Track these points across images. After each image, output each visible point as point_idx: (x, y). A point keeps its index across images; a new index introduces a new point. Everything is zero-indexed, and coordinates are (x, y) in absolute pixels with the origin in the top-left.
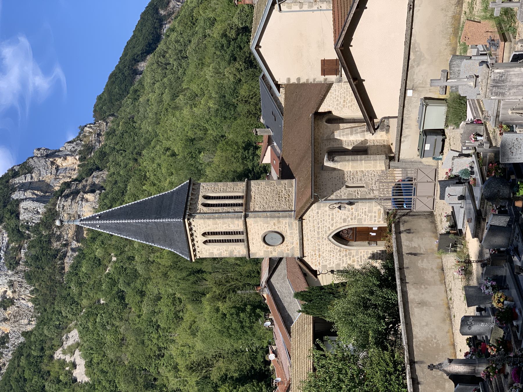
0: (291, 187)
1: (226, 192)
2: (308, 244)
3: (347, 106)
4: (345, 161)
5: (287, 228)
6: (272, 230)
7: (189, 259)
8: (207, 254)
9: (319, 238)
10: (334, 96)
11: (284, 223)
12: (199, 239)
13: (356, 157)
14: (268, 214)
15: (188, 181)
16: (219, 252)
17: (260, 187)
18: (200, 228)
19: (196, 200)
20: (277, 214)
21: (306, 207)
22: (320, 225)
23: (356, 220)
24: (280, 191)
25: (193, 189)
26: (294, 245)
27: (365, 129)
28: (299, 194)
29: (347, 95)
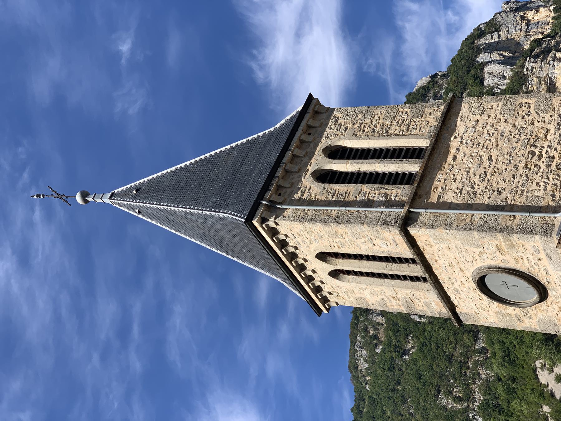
6: (497, 263)
11: (530, 250)
14: (478, 215)
20: (503, 218)
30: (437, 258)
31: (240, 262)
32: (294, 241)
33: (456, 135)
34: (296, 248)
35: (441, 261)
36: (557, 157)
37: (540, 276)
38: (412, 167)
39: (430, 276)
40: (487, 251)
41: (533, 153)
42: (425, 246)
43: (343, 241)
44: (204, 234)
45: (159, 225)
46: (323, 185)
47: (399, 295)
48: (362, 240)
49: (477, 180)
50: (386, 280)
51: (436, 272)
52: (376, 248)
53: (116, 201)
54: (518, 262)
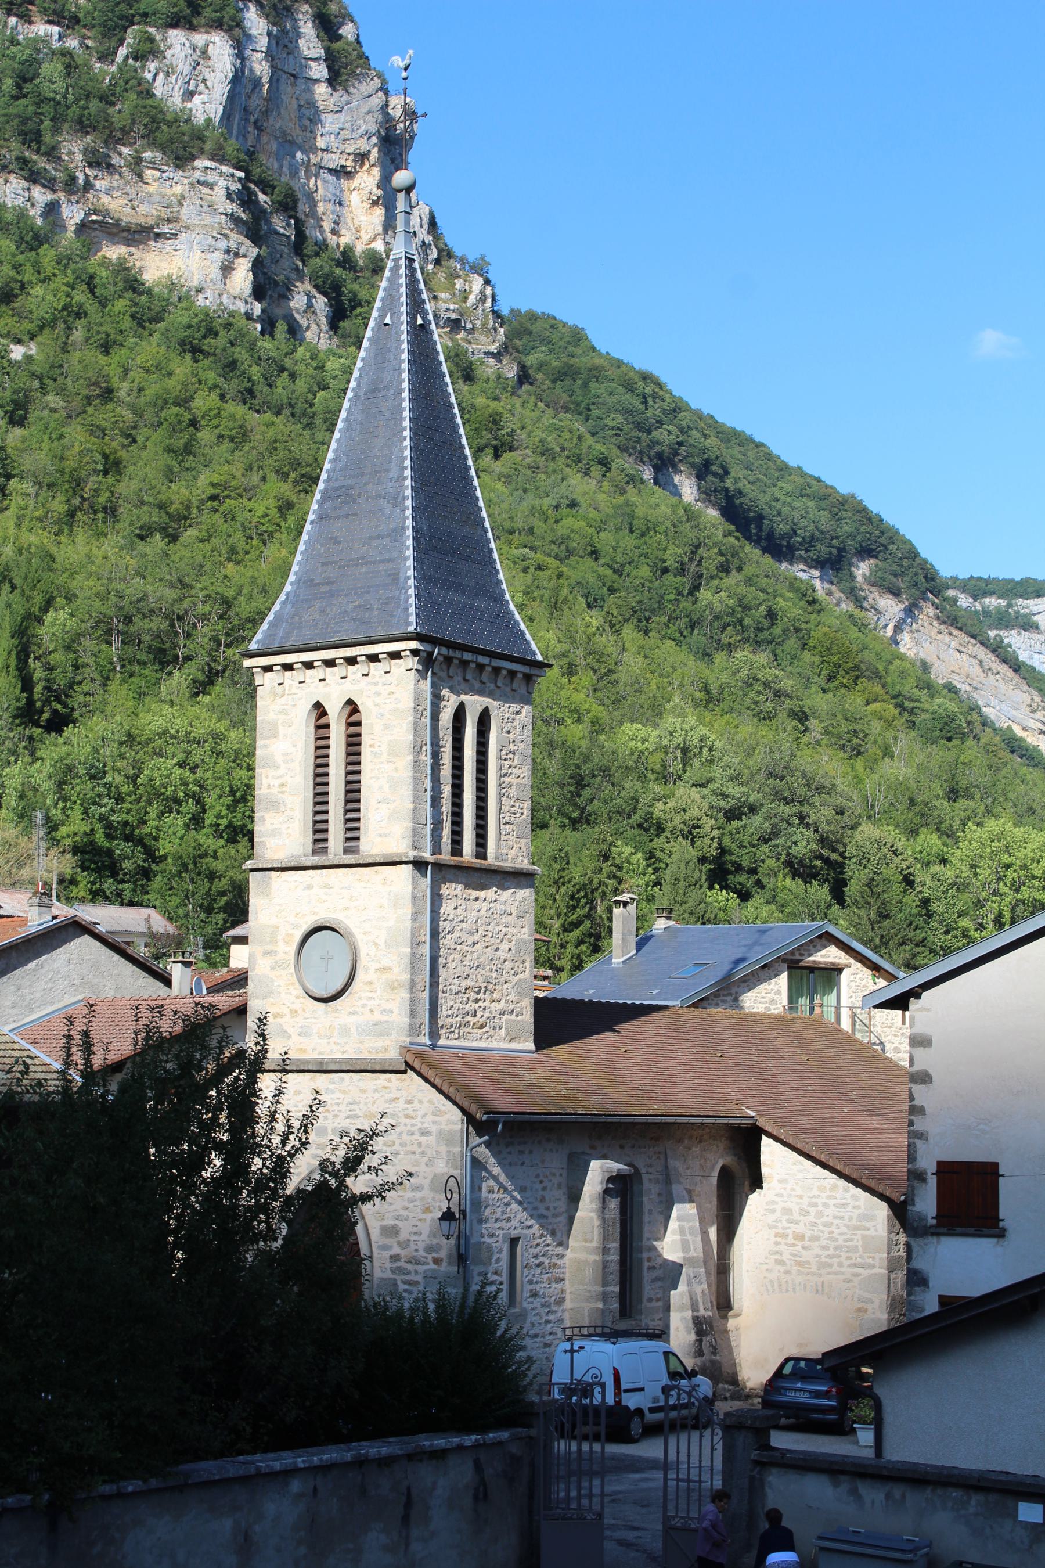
0: (508, 1034)
1: (501, 796)
3: (782, 1247)
4: (605, 1238)
7: (253, 646)
8: (272, 716)
10: (819, 1201)
11: (388, 1006)
12: (333, 688)
13: (615, 1277)
14: (426, 949)
15: (539, 657)
16: (279, 759)
17: (511, 919)
18: (378, 694)
19: (477, 685)
21: (452, 1092)
23: (389, 1275)
24: (496, 995)
25: (512, 674)
26: (295, 1038)
27: (702, 1312)
28: (478, 1060)
29: (825, 1248)
36: (476, 1019)
41: (478, 993)
49: (456, 934)
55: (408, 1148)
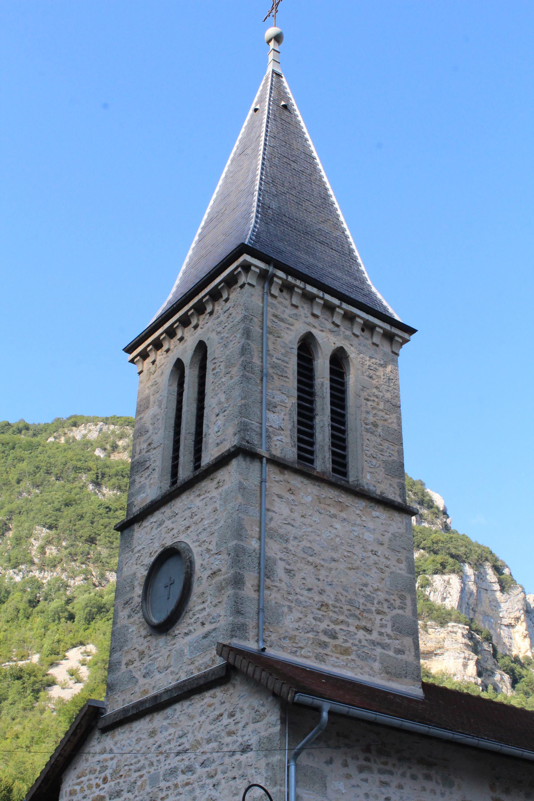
2: (139, 740)
5: (201, 631)
9: (154, 779)
22: (200, 771)
26: (142, 681)
30: (202, 497)
31: (193, 245)
32: (220, 311)
33: (364, 518)
34: (211, 313)
35: (198, 502)
37: (182, 625)
38: (323, 461)
39: (178, 489)
40: (212, 558)
42: (216, 481)
43: (222, 375)
44: (229, 195)
45: (240, 136)
46: (296, 346)
47: (154, 452)
48: (223, 400)
50: (172, 434)
51: (184, 497)
52: (213, 418)
53: (270, 80)
54: (199, 597)
55: (230, 774)
